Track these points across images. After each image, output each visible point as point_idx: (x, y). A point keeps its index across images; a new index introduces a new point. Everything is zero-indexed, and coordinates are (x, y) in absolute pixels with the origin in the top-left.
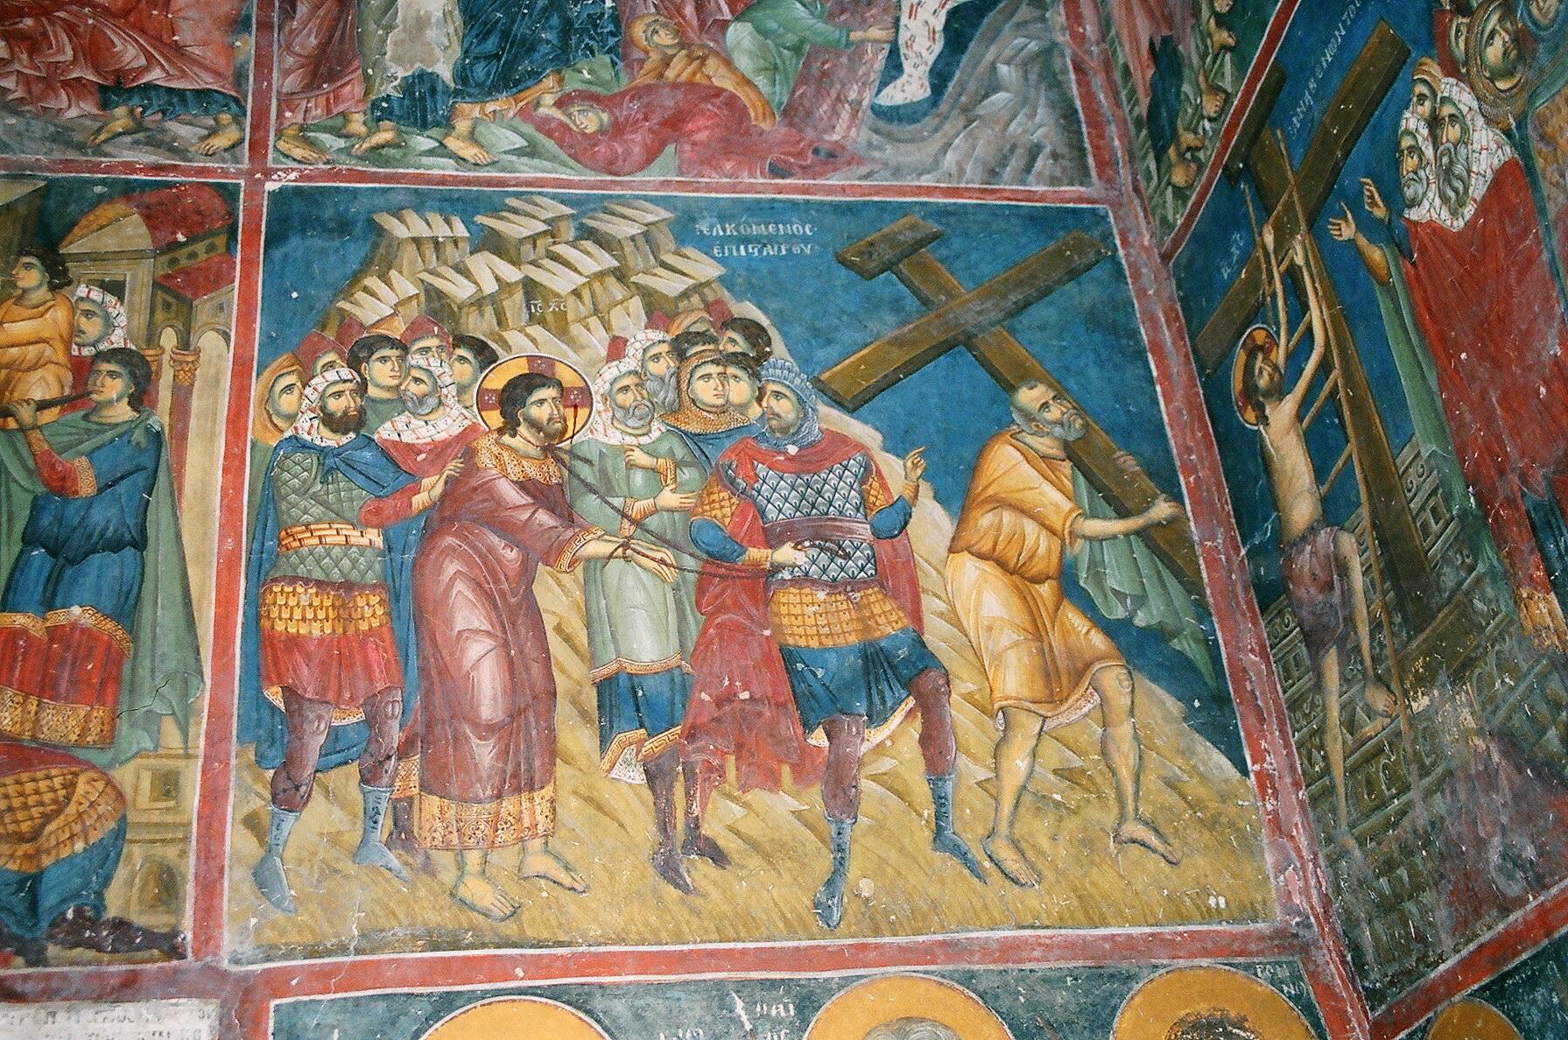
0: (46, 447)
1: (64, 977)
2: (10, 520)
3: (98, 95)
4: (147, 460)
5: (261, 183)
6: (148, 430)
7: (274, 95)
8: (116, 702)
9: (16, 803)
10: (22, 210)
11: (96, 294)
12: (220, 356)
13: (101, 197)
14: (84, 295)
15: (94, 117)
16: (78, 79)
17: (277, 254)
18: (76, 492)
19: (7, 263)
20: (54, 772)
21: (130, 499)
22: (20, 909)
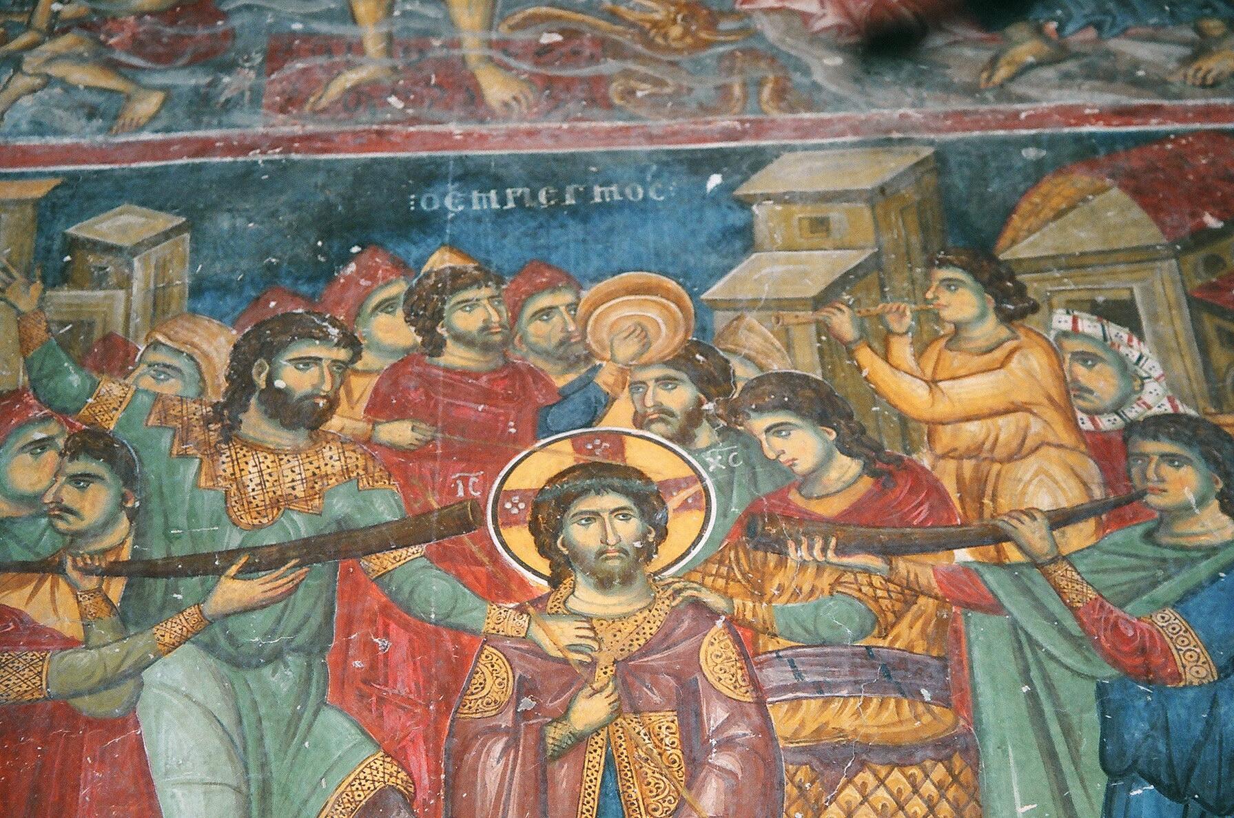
0: (1092, 594)
2: (1067, 732)
10: (909, 192)
11: (1088, 325)
13: (1039, 165)
18: (1178, 676)
19: (913, 282)
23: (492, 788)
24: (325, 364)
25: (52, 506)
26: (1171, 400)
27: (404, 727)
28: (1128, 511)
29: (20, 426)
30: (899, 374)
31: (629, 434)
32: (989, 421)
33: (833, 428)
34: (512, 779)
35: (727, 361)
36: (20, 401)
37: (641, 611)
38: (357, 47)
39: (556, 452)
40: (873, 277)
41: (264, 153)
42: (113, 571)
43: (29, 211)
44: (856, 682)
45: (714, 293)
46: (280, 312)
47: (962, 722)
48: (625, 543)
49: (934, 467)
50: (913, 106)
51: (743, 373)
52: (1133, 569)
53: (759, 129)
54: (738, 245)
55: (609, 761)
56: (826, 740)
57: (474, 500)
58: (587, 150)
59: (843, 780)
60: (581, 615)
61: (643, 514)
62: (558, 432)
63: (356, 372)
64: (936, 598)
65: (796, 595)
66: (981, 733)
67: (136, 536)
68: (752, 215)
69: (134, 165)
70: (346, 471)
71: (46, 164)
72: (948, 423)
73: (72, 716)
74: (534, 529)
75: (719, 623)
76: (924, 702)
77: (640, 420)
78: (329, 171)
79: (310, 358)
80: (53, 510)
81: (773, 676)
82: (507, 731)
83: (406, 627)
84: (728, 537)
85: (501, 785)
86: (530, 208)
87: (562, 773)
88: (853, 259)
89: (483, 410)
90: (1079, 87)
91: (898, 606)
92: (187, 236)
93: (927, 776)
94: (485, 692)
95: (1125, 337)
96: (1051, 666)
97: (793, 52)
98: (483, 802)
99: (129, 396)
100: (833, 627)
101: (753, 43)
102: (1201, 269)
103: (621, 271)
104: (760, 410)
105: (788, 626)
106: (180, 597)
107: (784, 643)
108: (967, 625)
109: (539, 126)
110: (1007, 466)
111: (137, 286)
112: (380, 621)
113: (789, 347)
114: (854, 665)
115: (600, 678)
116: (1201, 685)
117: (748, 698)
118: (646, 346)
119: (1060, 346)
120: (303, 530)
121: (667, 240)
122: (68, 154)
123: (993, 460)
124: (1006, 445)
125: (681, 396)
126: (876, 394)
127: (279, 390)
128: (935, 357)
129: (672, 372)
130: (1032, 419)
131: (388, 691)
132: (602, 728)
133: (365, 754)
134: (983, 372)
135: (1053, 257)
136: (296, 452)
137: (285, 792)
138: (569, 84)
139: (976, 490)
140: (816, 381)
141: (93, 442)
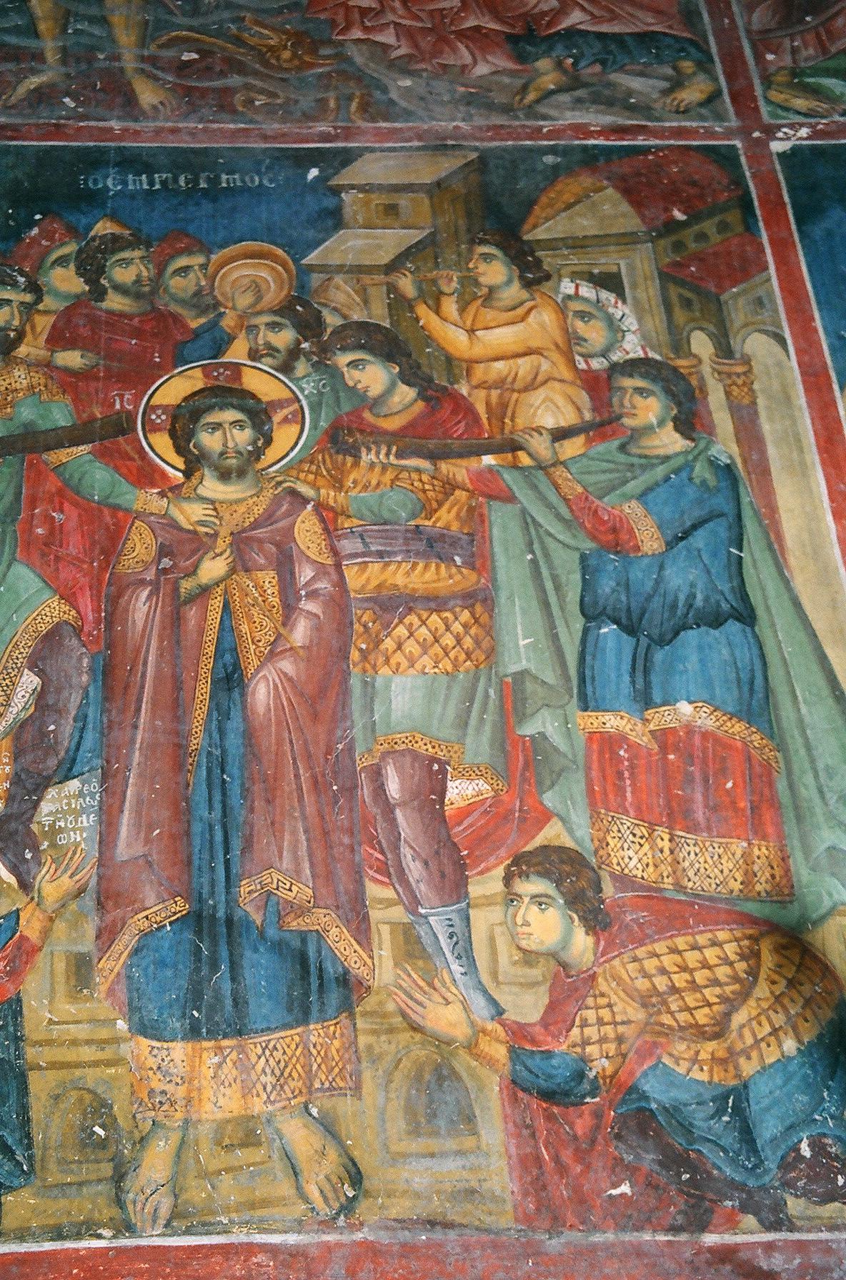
0: (580, 489)
1: (826, 1248)
2: (558, 588)
3: (508, 47)
4: (721, 502)
5: (762, 144)
6: (713, 463)
7: (742, 34)
8: (781, 836)
9: (680, 980)
10: (458, 186)
11: (587, 291)
12: (779, 364)
13: (556, 168)
14: (571, 291)
15: (512, 73)
16: (477, 29)
17: (817, 231)
18: (637, 548)
19: (459, 255)
20: (722, 935)
21: (714, 555)
22: (730, 1139)
23: (140, 624)
24: (15, 305)
26: (643, 348)
27: (75, 578)
28: (608, 429)
32: (512, 361)
37: (251, 497)
38: (39, 57)
39: (190, 377)
40: (429, 251)
44: (408, 551)
47: (483, 581)
48: (241, 448)
49: (470, 395)
50: (464, 120)
51: (332, 320)
52: (611, 471)
53: (348, 134)
54: (330, 223)
55: (226, 606)
56: (384, 592)
57: (129, 412)
59: (396, 621)
61: (254, 426)
63: (39, 311)
64: (467, 490)
65: (365, 488)
68: (342, 200)
74: (173, 434)
75: (309, 507)
77: (254, 355)
81: (347, 546)
82: (151, 582)
83: (76, 505)
84: (318, 443)
85: (146, 621)
87: (192, 613)
88: (415, 236)
91: (440, 496)
93: (456, 618)
95: (613, 301)
96: (548, 540)
97: (375, 75)
100: (392, 511)
101: (344, 66)
102: (669, 252)
104: (344, 349)
107: (356, 522)
108: (490, 510)
109: (181, 125)
112: (56, 499)
113: (366, 302)
114: (406, 539)
115: (221, 545)
117: (330, 562)
118: (259, 298)
119: (566, 306)
123: (513, 390)
125: (284, 338)
126: (429, 339)
129: (277, 319)
130: (543, 360)
132: (221, 581)
133: (45, 596)
135: (562, 239)
138: (204, 92)
139: (500, 412)
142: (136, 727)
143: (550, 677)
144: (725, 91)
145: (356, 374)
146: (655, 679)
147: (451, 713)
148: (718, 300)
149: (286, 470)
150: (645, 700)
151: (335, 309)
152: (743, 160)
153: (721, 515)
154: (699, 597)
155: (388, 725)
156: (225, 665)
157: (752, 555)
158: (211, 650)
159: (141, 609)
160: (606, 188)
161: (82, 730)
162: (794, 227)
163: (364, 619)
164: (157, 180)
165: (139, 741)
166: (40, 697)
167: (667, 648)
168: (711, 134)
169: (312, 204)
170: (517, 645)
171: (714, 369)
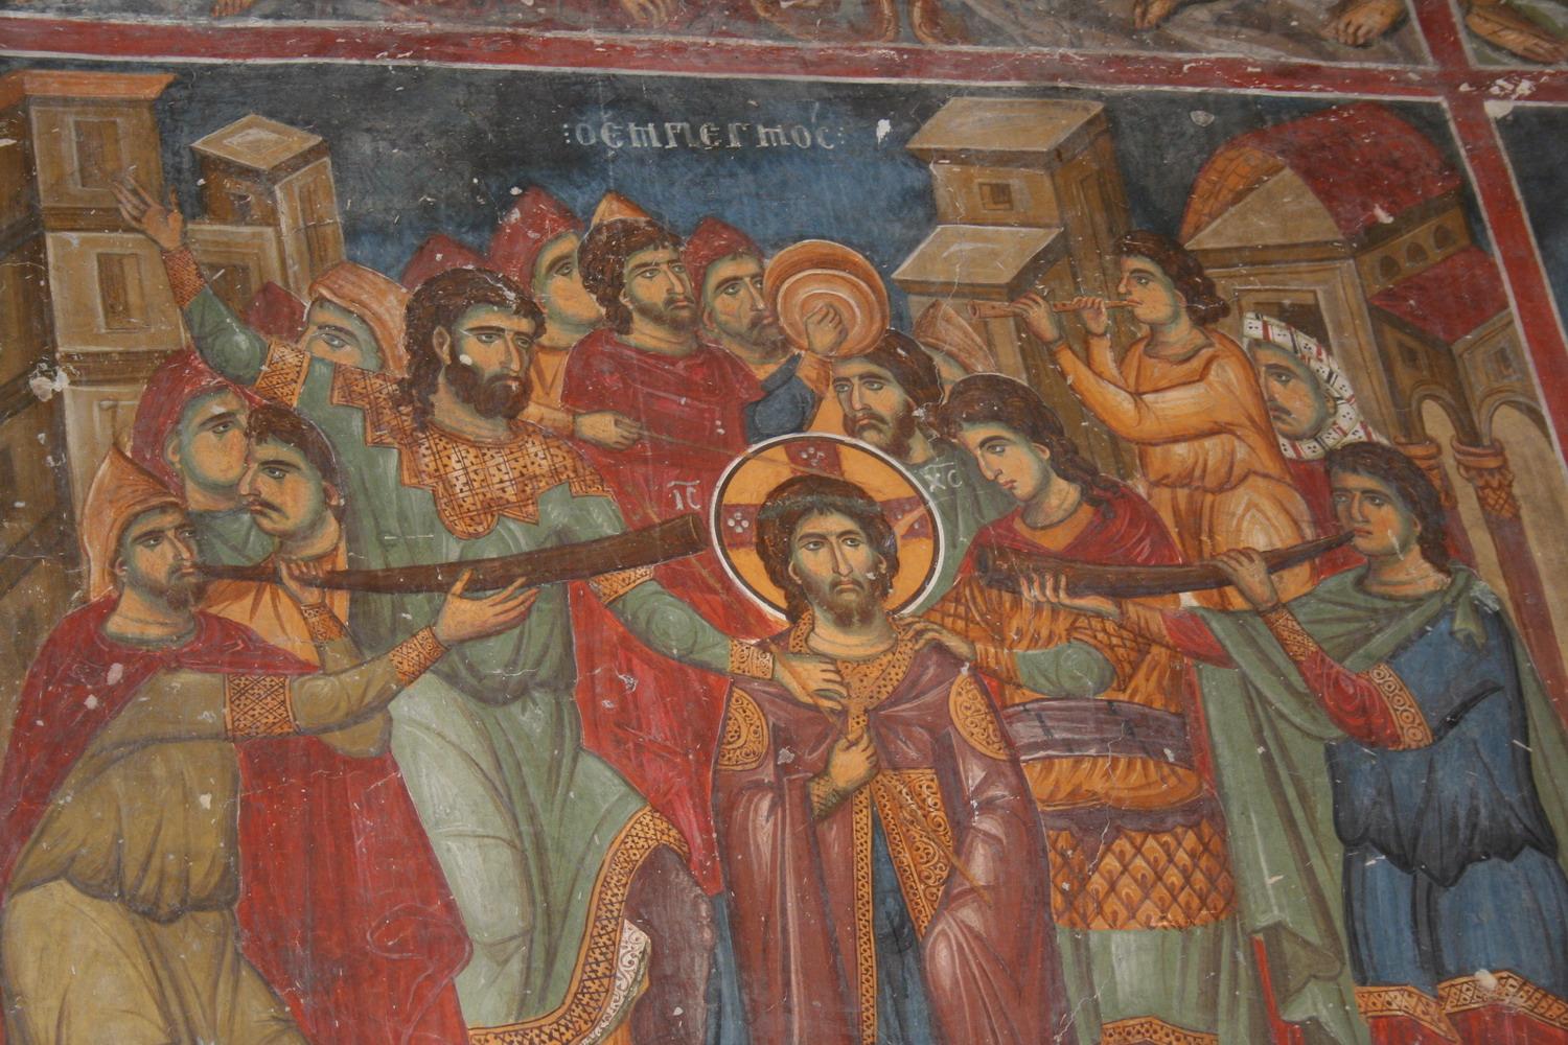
2: (1303, 797)
4: (1493, 669)
6: (1477, 609)
11: (1279, 334)
13: (1209, 130)
14: (1258, 333)
18: (1396, 739)
19: (1104, 272)
23: (766, 850)
24: (508, 336)
25: (251, 499)
26: (1364, 427)
29: (194, 397)
30: (1104, 384)
31: (842, 442)
32: (1196, 444)
33: (1046, 445)
34: (783, 840)
35: (930, 359)
36: (187, 364)
37: (885, 653)
41: (393, 56)
42: (332, 582)
43: (146, 115)
44: (1103, 741)
45: (904, 272)
46: (449, 267)
47: (1206, 786)
48: (857, 574)
49: (1150, 496)
50: (1072, 45)
51: (950, 374)
53: (919, 62)
55: (876, 823)
57: (695, 514)
58: (740, 76)
59: (1102, 847)
60: (824, 655)
62: (769, 436)
63: (543, 348)
64: (1167, 646)
65: (1034, 642)
66: (1224, 797)
67: (349, 541)
68: (931, 176)
69: (250, 61)
70: (555, 473)
71: (152, 53)
72: (1156, 445)
73: (327, 754)
74: (763, 554)
75: (965, 670)
76: (1168, 763)
77: (852, 426)
78: (469, 85)
79: (491, 328)
80: (252, 503)
81: (1025, 732)
82: (771, 787)
83: (648, 662)
84: (959, 571)
85: (774, 847)
86: (694, 150)
87: (832, 833)
88: (1041, 238)
89: (686, 405)
90: (1237, 34)
91: (1133, 656)
92: (327, 160)
93: (1180, 844)
94: (741, 742)
95: (1314, 349)
96: (1281, 725)
98: (760, 865)
99: (305, 365)
100: (1073, 678)
102: (1378, 271)
103: (802, 238)
104: (972, 419)
105: (1031, 677)
106: (409, 617)
108: (1200, 678)
109: (686, 39)
110: (1218, 498)
111: (285, 222)
112: (620, 653)
113: (990, 343)
114: (1098, 722)
115: (855, 728)
116: (1418, 748)
118: (843, 333)
119: (1254, 356)
120: (522, 541)
121: (845, 200)
122: (172, 40)
123: (1206, 491)
124: (1216, 471)
125: (889, 399)
126: (1083, 406)
127: (465, 367)
128: (1135, 363)
131: (644, 738)
132: (864, 784)
134: (1184, 384)
135: (1238, 249)
136: (499, 446)
137: (560, 849)
139: (1195, 523)
140: (1023, 387)
141: (274, 421)
142: (788, 1010)
143: (1313, 935)
144: (1413, 15)
145: (991, 457)
146: (1445, 935)
147: (1193, 987)
148: (1450, 352)
149: (926, 613)
150: (1436, 969)
151: (950, 355)
152: (1453, 127)
153: (1497, 689)
154: (1483, 812)
155: (1115, 1006)
156: (888, 915)
157: (1542, 749)
158: (866, 891)
159: (763, 825)
160: (1282, 168)
161: (719, 1014)
162: (1533, 241)
163: (1061, 843)
164: (670, 133)
165: (796, 1032)
166: (654, 959)
167: (1452, 889)
168: (1408, 87)
169: (893, 178)
170: (1263, 886)
171: (1459, 463)
